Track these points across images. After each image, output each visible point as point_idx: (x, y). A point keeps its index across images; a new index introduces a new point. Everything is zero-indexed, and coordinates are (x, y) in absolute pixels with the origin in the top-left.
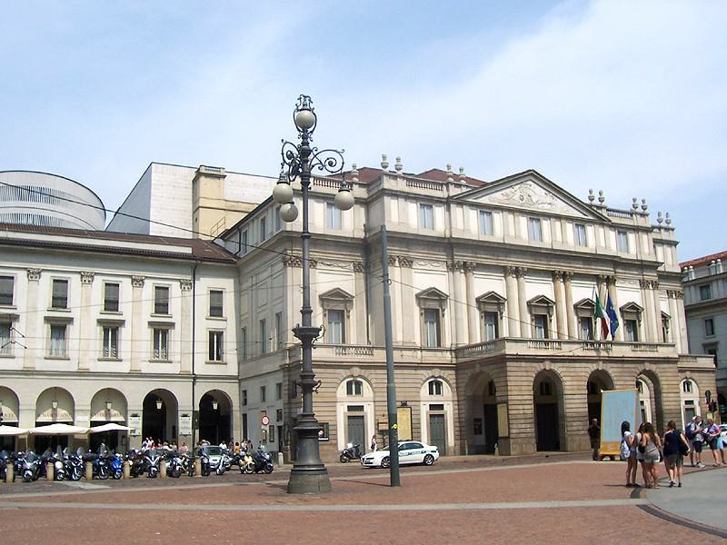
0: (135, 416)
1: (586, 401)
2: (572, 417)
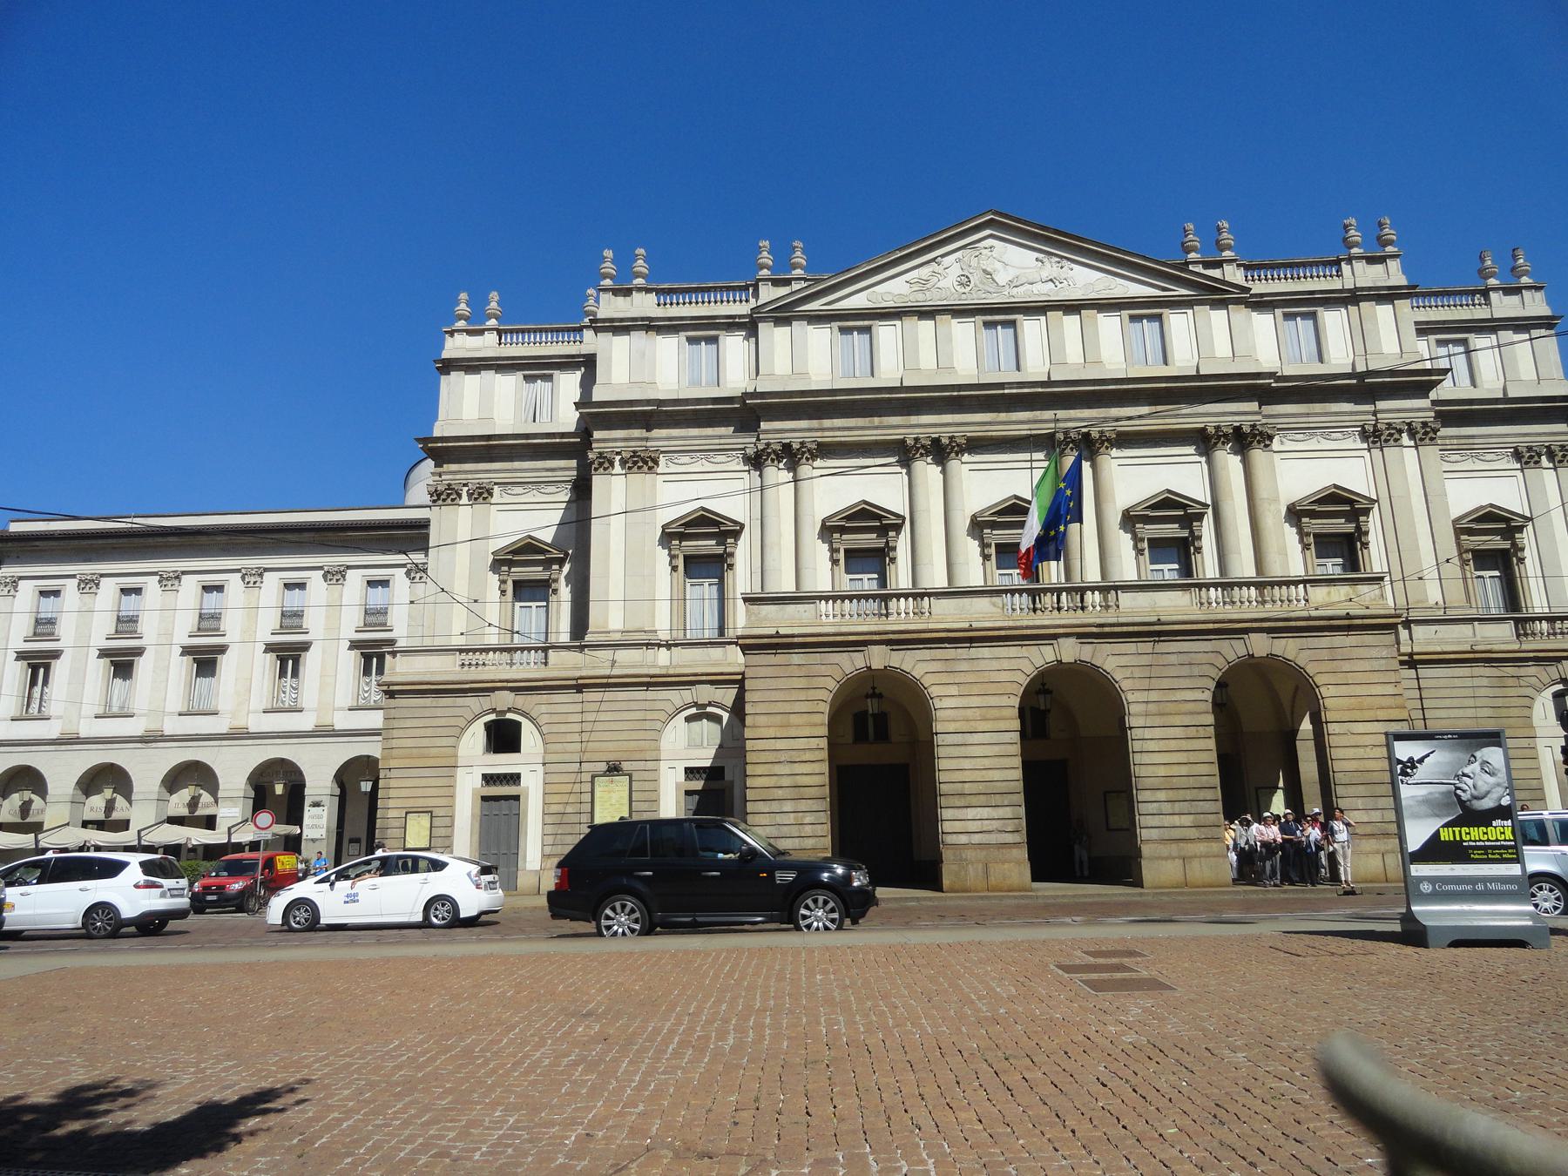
0: (316, 805)
1: (1016, 749)
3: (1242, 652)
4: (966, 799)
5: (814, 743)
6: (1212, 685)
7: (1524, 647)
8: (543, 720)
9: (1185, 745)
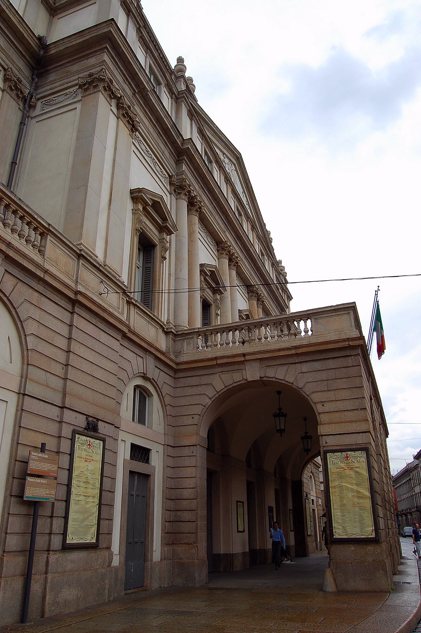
8: (31, 327)
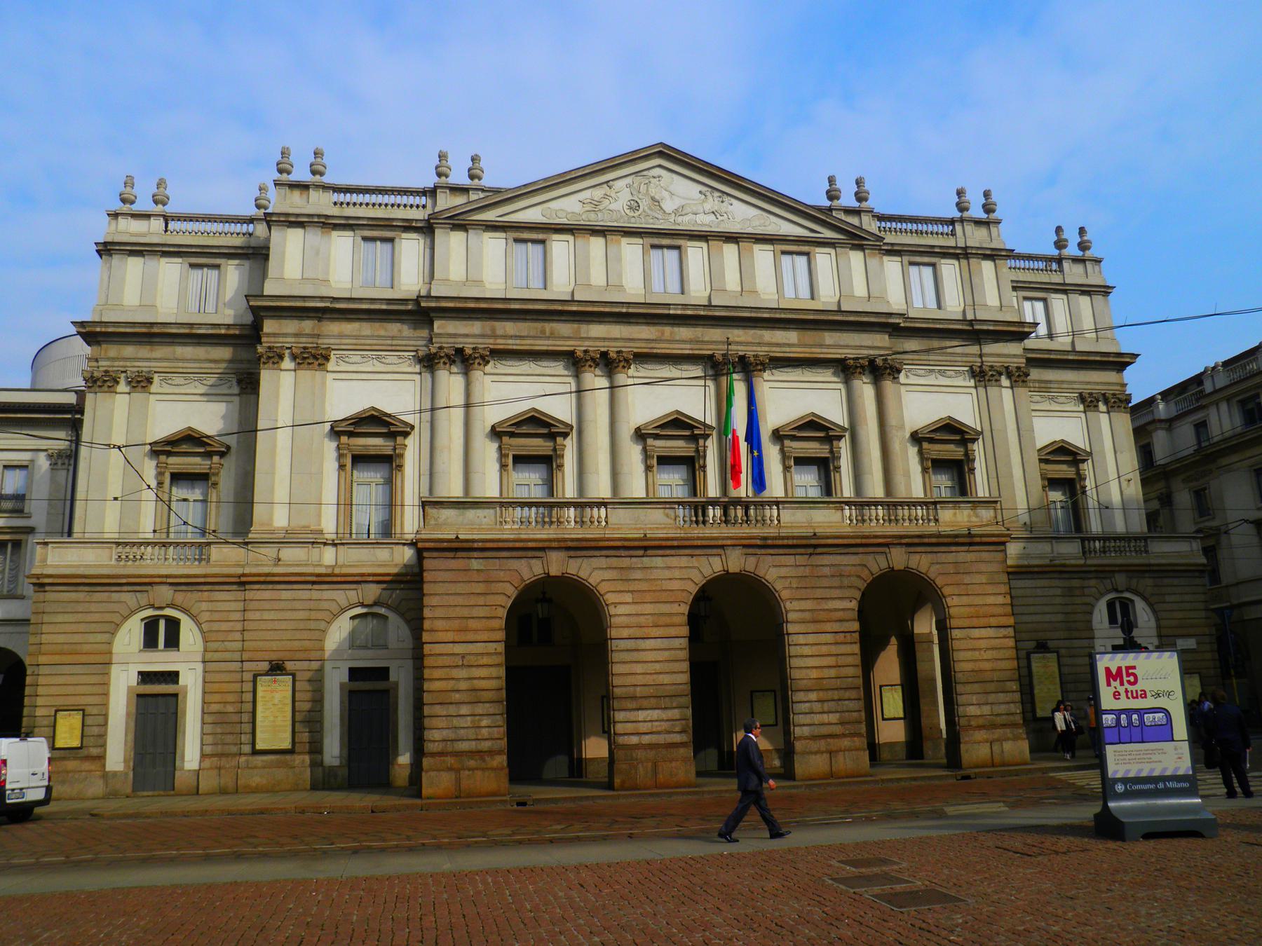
1: (684, 654)
2: (634, 698)
3: (884, 565)
4: (638, 701)
5: (491, 647)
6: (858, 595)
7: (1089, 562)
8: (204, 617)
9: (834, 650)
